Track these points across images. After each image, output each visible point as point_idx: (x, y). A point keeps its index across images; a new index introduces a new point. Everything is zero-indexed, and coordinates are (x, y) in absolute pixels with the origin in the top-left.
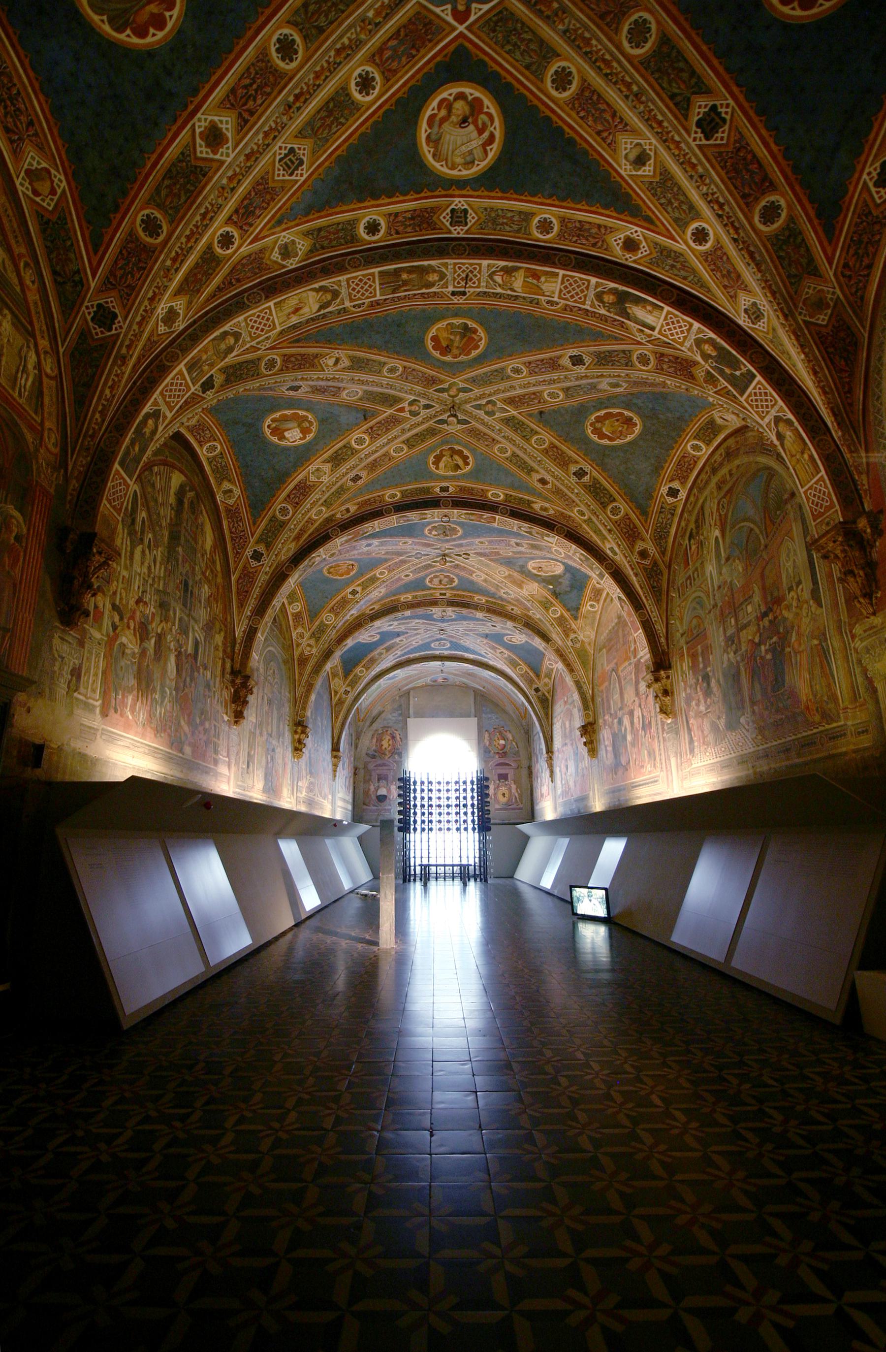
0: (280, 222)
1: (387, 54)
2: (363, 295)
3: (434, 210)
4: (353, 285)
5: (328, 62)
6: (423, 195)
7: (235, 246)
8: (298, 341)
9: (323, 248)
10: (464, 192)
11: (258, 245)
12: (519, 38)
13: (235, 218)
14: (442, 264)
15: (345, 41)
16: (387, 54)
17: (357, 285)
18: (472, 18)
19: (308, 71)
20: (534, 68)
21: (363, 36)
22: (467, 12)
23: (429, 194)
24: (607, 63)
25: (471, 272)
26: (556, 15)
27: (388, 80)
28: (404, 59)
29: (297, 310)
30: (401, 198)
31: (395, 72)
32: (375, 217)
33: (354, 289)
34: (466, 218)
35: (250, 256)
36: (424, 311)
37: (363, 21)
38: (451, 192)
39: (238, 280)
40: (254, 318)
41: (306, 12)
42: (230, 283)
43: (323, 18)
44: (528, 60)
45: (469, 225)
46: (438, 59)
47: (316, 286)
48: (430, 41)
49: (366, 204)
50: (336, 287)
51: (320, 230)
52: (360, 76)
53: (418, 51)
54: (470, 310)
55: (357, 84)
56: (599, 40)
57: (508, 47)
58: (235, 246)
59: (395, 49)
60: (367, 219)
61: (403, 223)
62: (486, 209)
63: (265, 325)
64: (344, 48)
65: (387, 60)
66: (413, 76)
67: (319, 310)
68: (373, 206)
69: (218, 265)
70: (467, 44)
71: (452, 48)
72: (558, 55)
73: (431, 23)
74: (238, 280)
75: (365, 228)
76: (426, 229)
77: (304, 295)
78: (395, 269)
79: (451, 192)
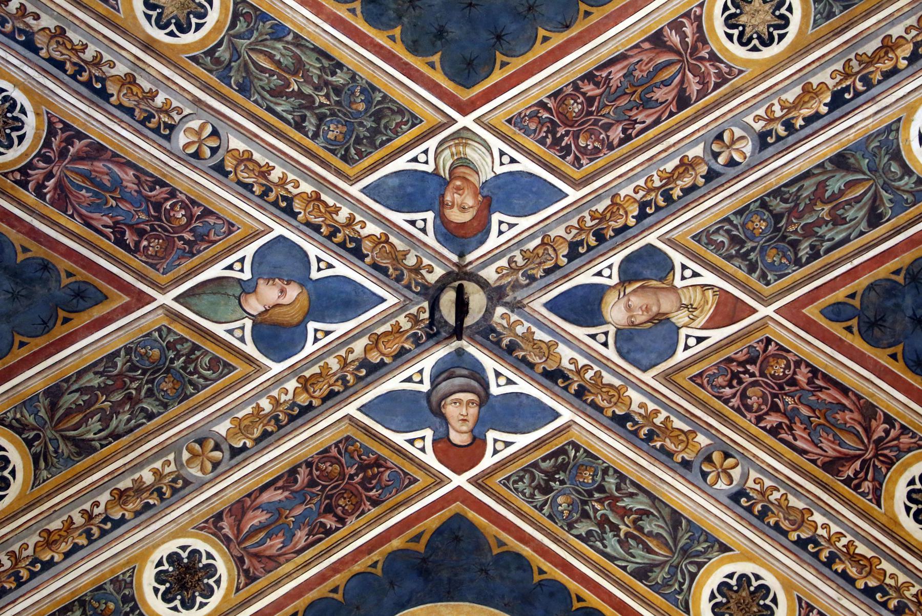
1: (257, 518)
5: (89, 516)
12: (612, 507)
15: (147, 476)
16: (257, 518)
18: (488, 461)
19: (27, 529)
20: (660, 575)
21: (194, 471)
22: (477, 446)
24: (867, 565)
26: (709, 459)
27: (251, 579)
28: (301, 537)
31: (274, 561)
37: (201, 442)
41: (53, 408)
43: (95, 424)
44: (641, 557)
46: (396, 543)
48: (375, 503)
52: (173, 558)
53: (342, 521)
55: (160, 578)
56: (828, 512)
57: (583, 528)
59: (277, 510)
64: (139, 489)
65: (255, 531)
66: (322, 577)
70: (472, 515)
71: (433, 523)
72: (724, 548)
73: (378, 462)
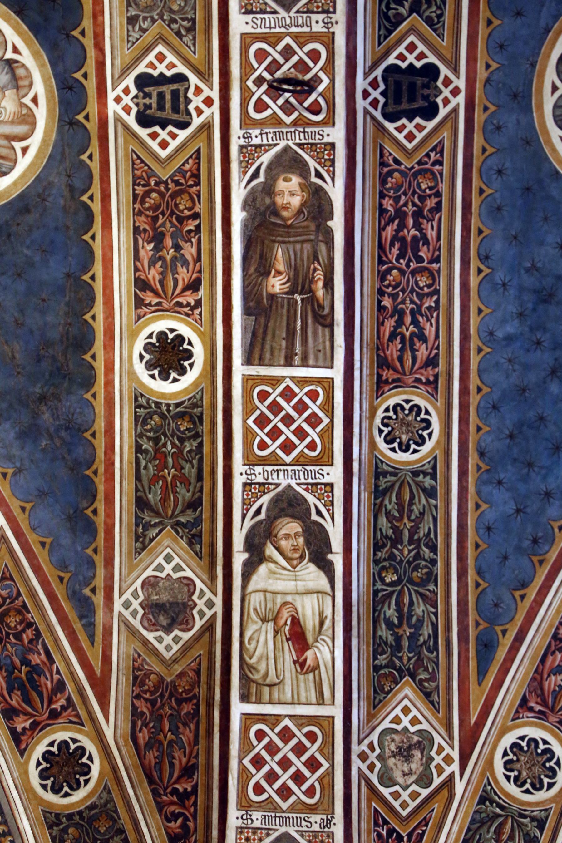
0: (86, 609)
2: (313, 420)
3: (142, 179)
4: (274, 446)
6: (96, 207)
7: (91, 747)
8: (487, 647)
9: (195, 504)
10: (91, 85)
11: (119, 686)
13: (21, 724)
14: (245, 165)
17: (275, 433)
23: (96, 189)
25: (274, 66)
29: (298, 637)
30: (98, 269)
32: (139, 346)
33: (288, 447)
34: (162, 80)
35: (135, 714)
36: (495, 211)
38: (92, 126)
39: (188, 771)
40: (259, 776)
42: (183, 797)
45: (181, 69)
47: (239, 558)
49: (100, 366)
50: (265, 500)
51: (141, 503)
54: (498, 47)
58: (91, 747)
60: (140, 369)
61: (170, 268)
62: (132, 21)
63: (299, 750)
67: (327, 568)
68: (109, 346)
69: (112, 816)
74: (188, 771)
75: (165, 376)
76: (195, 199)
77: (255, 600)
78: (247, 311)
79: (92, 126)
